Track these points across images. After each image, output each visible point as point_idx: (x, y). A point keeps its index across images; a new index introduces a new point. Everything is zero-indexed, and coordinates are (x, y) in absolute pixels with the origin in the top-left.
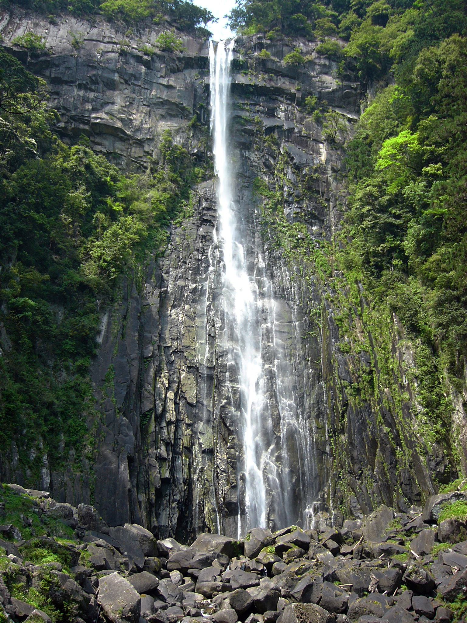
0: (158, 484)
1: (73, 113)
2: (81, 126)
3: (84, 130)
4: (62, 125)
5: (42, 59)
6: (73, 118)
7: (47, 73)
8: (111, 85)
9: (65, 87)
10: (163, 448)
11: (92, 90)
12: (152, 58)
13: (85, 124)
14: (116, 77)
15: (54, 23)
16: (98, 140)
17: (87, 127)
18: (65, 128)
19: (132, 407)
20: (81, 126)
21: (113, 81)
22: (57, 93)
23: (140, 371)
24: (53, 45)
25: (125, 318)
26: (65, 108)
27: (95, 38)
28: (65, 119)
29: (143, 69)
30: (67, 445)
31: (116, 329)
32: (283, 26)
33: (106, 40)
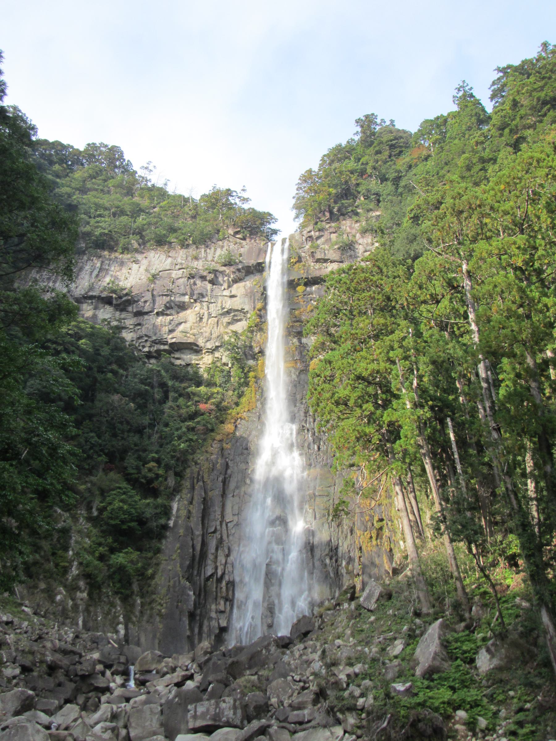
0: (217, 631)
1: (154, 338)
2: (162, 347)
3: (165, 350)
4: (146, 349)
5: (124, 299)
6: (155, 342)
7: (130, 309)
8: (182, 307)
9: (146, 317)
10: (222, 602)
11: (167, 315)
12: (215, 275)
13: (165, 344)
14: (186, 299)
15: (136, 262)
16: (177, 355)
17: (166, 347)
18: (149, 352)
19: (195, 572)
20: (162, 347)
21: (184, 302)
22: (139, 324)
23: (204, 544)
24: (133, 283)
25: (191, 503)
26: (146, 336)
27: (168, 268)
28: (148, 344)
29: (209, 286)
30: (142, 605)
31: (184, 513)
32: (331, 212)
33: (178, 267)
